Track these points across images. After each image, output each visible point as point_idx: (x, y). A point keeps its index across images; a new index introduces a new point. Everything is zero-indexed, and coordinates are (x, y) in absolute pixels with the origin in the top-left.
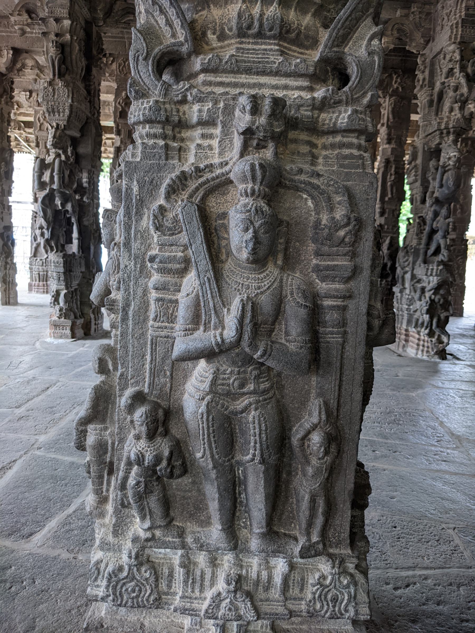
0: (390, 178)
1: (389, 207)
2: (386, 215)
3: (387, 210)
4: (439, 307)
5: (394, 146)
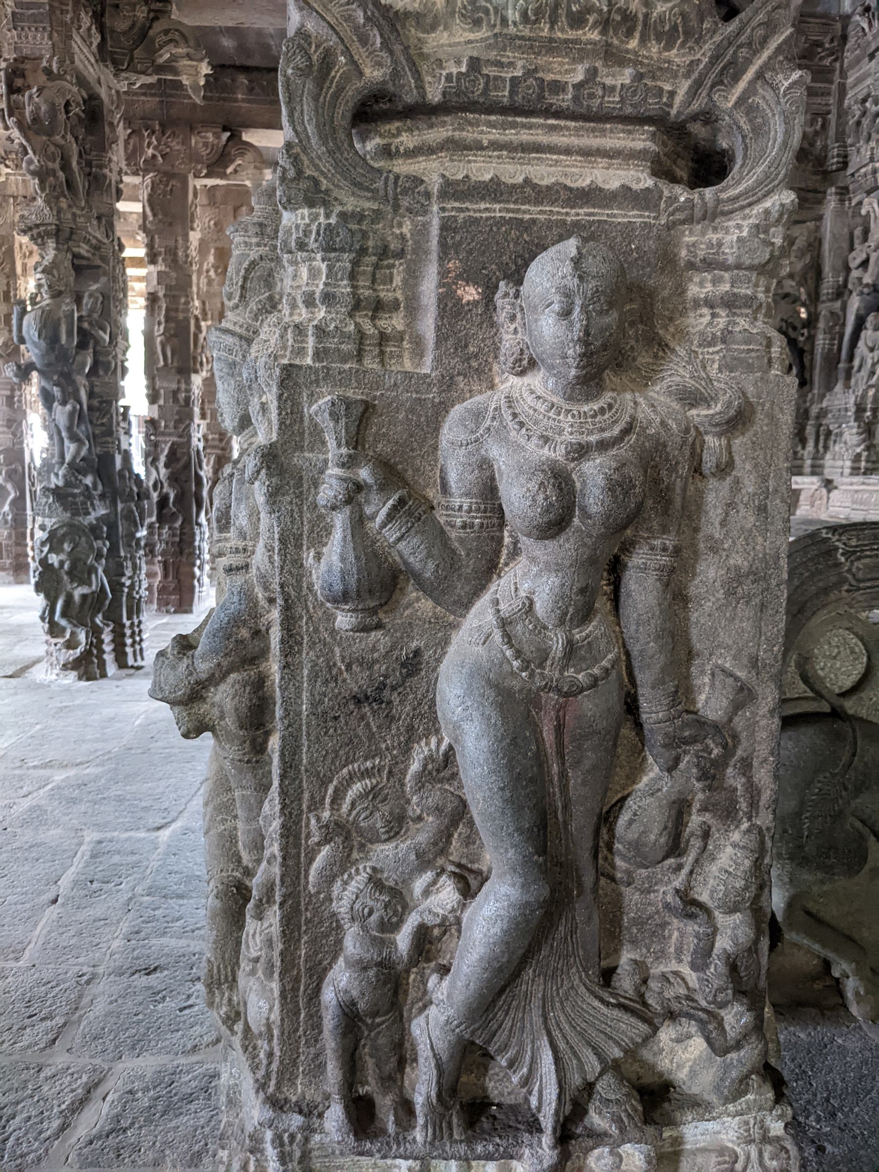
0: (158, 330)
1: (165, 385)
2: (161, 402)
3: (162, 392)
4: (65, 577)
5: (163, 268)
